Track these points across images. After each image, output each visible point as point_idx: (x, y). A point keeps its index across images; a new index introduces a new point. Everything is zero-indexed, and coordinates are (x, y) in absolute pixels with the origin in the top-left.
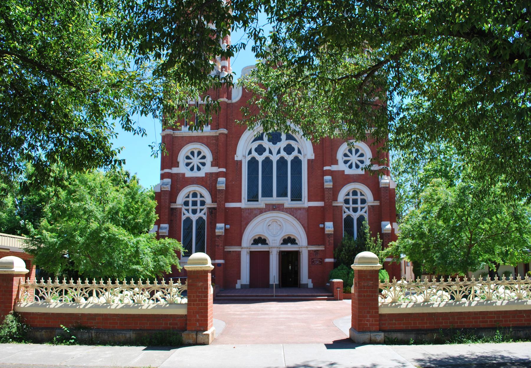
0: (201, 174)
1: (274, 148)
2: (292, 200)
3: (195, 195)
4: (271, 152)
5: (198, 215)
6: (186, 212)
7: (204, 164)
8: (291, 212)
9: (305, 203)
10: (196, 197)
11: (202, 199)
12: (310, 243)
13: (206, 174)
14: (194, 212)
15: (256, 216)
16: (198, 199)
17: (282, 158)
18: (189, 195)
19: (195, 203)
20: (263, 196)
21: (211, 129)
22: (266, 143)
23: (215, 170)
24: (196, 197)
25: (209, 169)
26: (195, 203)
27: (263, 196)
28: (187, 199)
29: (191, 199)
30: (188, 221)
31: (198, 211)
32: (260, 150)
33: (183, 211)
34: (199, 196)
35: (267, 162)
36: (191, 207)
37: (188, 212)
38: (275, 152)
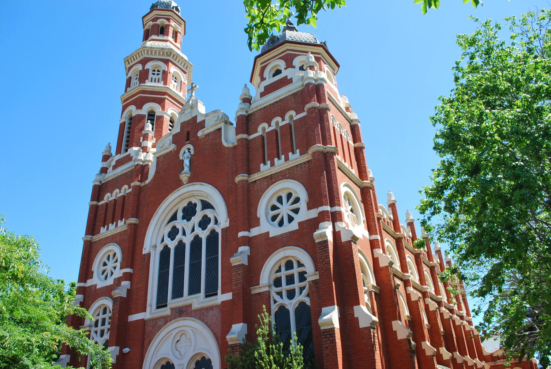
0: (294, 226)
3: (289, 265)
5: (299, 298)
6: (277, 298)
7: (296, 211)
10: (292, 268)
11: (301, 269)
13: (300, 224)
14: (291, 295)
16: (296, 271)
18: (280, 267)
19: (290, 280)
23: (314, 213)
24: (292, 268)
26: (290, 280)
28: (278, 275)
29: (284, 274)
30: (282, 312)
31: (297, 291)
34: (295, 265)
36: (285, 287)
37: (282, 297)
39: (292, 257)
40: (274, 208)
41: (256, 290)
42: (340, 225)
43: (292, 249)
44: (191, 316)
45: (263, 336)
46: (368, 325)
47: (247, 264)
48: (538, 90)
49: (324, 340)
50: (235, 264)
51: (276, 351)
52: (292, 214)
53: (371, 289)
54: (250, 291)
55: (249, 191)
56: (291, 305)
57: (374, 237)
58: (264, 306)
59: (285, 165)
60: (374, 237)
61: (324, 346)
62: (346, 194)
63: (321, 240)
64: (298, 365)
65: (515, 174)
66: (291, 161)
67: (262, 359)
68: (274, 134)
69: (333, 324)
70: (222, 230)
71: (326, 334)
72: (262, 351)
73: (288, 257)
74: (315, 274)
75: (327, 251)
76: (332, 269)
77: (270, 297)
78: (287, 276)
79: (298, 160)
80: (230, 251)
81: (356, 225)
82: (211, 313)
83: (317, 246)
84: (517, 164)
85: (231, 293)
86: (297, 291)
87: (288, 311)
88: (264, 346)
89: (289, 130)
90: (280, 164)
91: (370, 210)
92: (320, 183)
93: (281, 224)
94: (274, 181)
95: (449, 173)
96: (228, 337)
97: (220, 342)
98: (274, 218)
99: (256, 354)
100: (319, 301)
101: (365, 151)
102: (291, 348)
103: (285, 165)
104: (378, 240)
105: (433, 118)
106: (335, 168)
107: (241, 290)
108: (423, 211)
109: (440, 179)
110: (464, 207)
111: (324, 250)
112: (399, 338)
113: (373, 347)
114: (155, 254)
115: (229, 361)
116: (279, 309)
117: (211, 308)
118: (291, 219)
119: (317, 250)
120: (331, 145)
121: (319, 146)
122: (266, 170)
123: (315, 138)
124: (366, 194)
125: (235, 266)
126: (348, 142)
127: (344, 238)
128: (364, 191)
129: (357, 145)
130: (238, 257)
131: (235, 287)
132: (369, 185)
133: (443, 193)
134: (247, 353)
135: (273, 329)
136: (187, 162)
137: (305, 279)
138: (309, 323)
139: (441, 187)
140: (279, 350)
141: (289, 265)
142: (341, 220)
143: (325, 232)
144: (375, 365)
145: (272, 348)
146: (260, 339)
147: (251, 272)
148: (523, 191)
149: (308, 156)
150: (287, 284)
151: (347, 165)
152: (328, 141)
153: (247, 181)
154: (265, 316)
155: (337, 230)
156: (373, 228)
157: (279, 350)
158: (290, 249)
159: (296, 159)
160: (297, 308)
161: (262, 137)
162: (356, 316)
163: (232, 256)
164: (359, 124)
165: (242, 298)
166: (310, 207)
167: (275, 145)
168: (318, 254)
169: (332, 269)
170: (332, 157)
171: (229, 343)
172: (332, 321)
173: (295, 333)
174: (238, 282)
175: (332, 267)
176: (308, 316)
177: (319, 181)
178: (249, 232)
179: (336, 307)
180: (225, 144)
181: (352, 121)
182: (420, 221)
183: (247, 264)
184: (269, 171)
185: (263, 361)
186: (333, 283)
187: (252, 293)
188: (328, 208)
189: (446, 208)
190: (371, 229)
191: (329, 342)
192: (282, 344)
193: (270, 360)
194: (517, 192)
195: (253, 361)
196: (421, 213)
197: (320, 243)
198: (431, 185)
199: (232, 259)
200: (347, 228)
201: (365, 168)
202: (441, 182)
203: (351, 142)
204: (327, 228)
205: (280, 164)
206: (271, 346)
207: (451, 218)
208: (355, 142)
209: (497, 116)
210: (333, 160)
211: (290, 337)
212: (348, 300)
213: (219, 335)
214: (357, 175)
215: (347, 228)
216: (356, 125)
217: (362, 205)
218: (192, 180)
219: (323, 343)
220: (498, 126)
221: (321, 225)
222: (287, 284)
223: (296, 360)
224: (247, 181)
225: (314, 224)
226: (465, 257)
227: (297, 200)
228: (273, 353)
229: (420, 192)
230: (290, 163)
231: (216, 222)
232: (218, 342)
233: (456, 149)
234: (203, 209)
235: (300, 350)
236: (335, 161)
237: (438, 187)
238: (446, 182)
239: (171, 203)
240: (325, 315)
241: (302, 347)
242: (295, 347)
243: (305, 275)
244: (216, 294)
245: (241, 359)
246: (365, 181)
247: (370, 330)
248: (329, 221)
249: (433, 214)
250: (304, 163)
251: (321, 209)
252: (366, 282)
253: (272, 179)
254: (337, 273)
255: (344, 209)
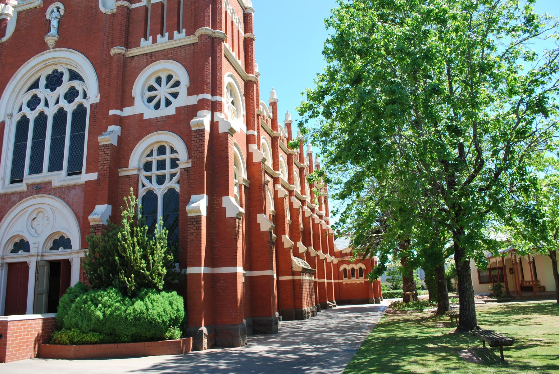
0: (171, 111)
3: (162, 150)
6: (146, 182)
7: (175, 95)
11: (174, 156)
13: (177, 109)
14: (161, 180)
16: (168, 157)
19: (161, 165)
21: (187, 35)
23: (193, 100)
26: (161, 165)
28: (149, 159)
29: (155, 158)
30: (150, 197)
31: (168, 177)
33: (142, 179)
34: (168, 150)
36: (155, 172)
37: (151, 182)
39: (166, 142)
40: (151, 89)
41: (123, 173)
42: (218, 116)
43: (167, 134)
44: (50, 194)
45: (128, 218)
46: (234, 215)
47: (116, 145)
48: (429, 11)
49: (190, 226)
50: (103, 144)
51: (140, 234)
52: (171, 98)
53: (242, 182)
54: (118, 173)
55: (125, 66)
56: (160, 191)
57: (251, 132)
58: (132, 189)
59: (168, 44)
60: (251, 132)
61: (189, 232)
62: (230, 85)
63: (197, 128)
64: (162, 248)
65: (392, 90)
66: (175, 40)
67: (125, 240)
68: (160, 7)
69: (200, 212)
70: (92, 105)
71: (192, 220)
72: (126, 233)
73: (161, 142)
74: (188, 162)
75: (203, 140)
76: (205, 159)
77: (138, 181)
78: (158, 162)
79: (183, 40)
80: (99, 129)
81: (235, 118)
82: (73, 192)
83: (193, 134)
84: (395, 81)
85: (97, 173)
87: (156, 196)
88: (129, 228)
89: (176, 6)
90: (163, 42)
91: (252, 105)
92: (204, 69)
93: (157, 106)
94: (154, 59)
95: (333, 79)
96: (90, 217)
97: (82, 222)
98: (150, 100)
99: (119, 235)
100: (188, 189)
101: (255, 43)
102: (156, 232)
103: (168, 44)
104: (254, 135)
105: (327, 21)
106: (221, 55)
107: (108, 171)
108: (302, 113)
109: (323, 84)
110: (341, 115)
111: (200, 138)
112: (261, 230)
113: (236, 236)
114: (11, 124)
115: (90, 240)
116: (147, 193)
117: (74, 187)
118: (168, 103)
119: (192, 138)
120: (221, 30)
121: (207, 29)
122: (146, 46)
123: (204, 20)
124: (249, 88)
125: (103, 146)
126: (238, 31)
127: (222, 129)
128: (248, 84)
129: (247, 35)
130: (107, 136)
131: (102, 167)
132: (253, 79)
133: (324, 98)
134: (110, 234)
135: (139, 212)
136: (54, 23)
137: (177, 166)
138: (177, 210)
139: (323, 92)
140: (144, 233)
141: (162, 150)
142: (221, 111)
143: (203, 121)
144: (236, 253)
145: (137, 231)
146: (125, 221)
147: (120, 153)
148: (395, 106)
149: (195, 38)
150: (158, 169)
151: (234, 54)
152: (218, 25)
153: (124, 55)
154: (132, 198)
155: (215, 120)
156: (252, 123)
157: (144, 233)
158: (164, 134)
159: (181, 39)
160: (166, 193)
161: (146, 8)
162: (223, 206)
163: (101, 134)
164: (253, 14)
165: (108, 179)
166: (191, 92)
167: (160, 20)
168: (193, 142)
169: (205, 159)
170: (220, 44)
171: (91, 224)
172: (199, 209)
173: (161, 218)
174: (105, 162)
175: (205, 157)
176: (175, 202)
177: (203, 66)
178: (122, 111)
179: (205, 196)
180: (102, 9)
181: (246, 9)
182: (298, 122)
183: (116, 145)
184: (150, 48)
185: (126, 242)
186: (205, 172)
187: (120, 174)
188: (208, 96)
189: (323, 113)
190: (249, 124)
191: (194, 228)
192: (147, 228)
193: (134, 242)
194: (389, 106)
195: (116, 242)
196: (300, 115)
197: (196, 131)
198: (314, 88)
199: (100, 138)
200: (225, 120)
201: (252, 61)
202: (324, 87)
203: (242, 32)
204: (205, 116)
206: (135, 229)
207: (327, 123)
208: (245, 32)
209: (387, 30)
210: (221, 46)
211: (155, 221)
212: (218, 190)
213: (81, 214)
214: (243, 67)
215: (225, 120)
216: (250, 14)
217: (244, 99)
218: (59, 45)
219: (189, 229)
220: (386, 41)
221: (200, 113)
222: (158, 169)
223: (160, 243)
224: (124, 55)
225: (192, 111)
226: (332, 162)
227: (177, 84)
228: (137, 236)
229: (302, 93)
230: (175, 42)
231: (85, 96)
232: (79, 223)
233: (343, 56)
234: (70, 80)
235: (165, 234)
236: (223, 48)
237: (320, 91)
238: (328, 88)
239: (33, 68)
240: (193, 203)
241: (167, 231)
242: (160, 231)
243: (177, 162)
244: (80, 173)
245: (104, 240)
246: (250, 75)
247: (235, 220)
248: (208, 109)
249: (311, 117)
250: (190, 45)
251: (201, 96)
252: (238, 174)
253: (152, 57)
254: (210, 163)
255: (225, 99)
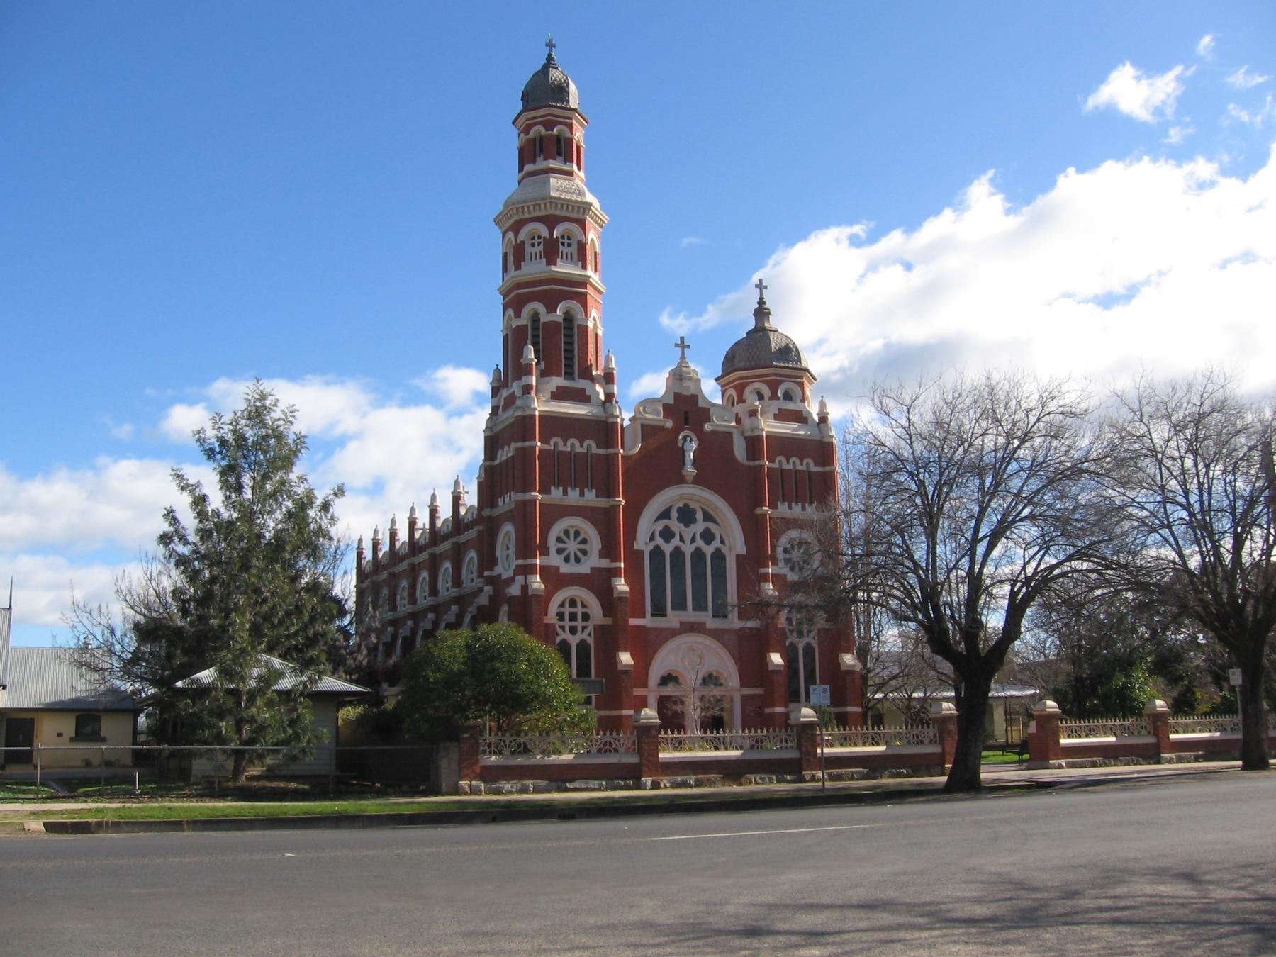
0: (584, 569)
1: (688, 532)
2: (714, 616)
4: (682, 539)
6: (560, 631)
8: (717, 634)
9: (734, 622)
12: (744, 683)
14: (573, 631)
15: (666, 640)
17: (698, 550)
19: (573, 617)
20: (674, 608)
22: (676, 526)
23: (605, 563)
25: (594, 561)
27: (674, 608)
31: (580, 629)
32: (667, 534)
35: (677, 554)
38: (688, 539)
56: (573, 641)
86: (580, 629)
205: (573, 497)
